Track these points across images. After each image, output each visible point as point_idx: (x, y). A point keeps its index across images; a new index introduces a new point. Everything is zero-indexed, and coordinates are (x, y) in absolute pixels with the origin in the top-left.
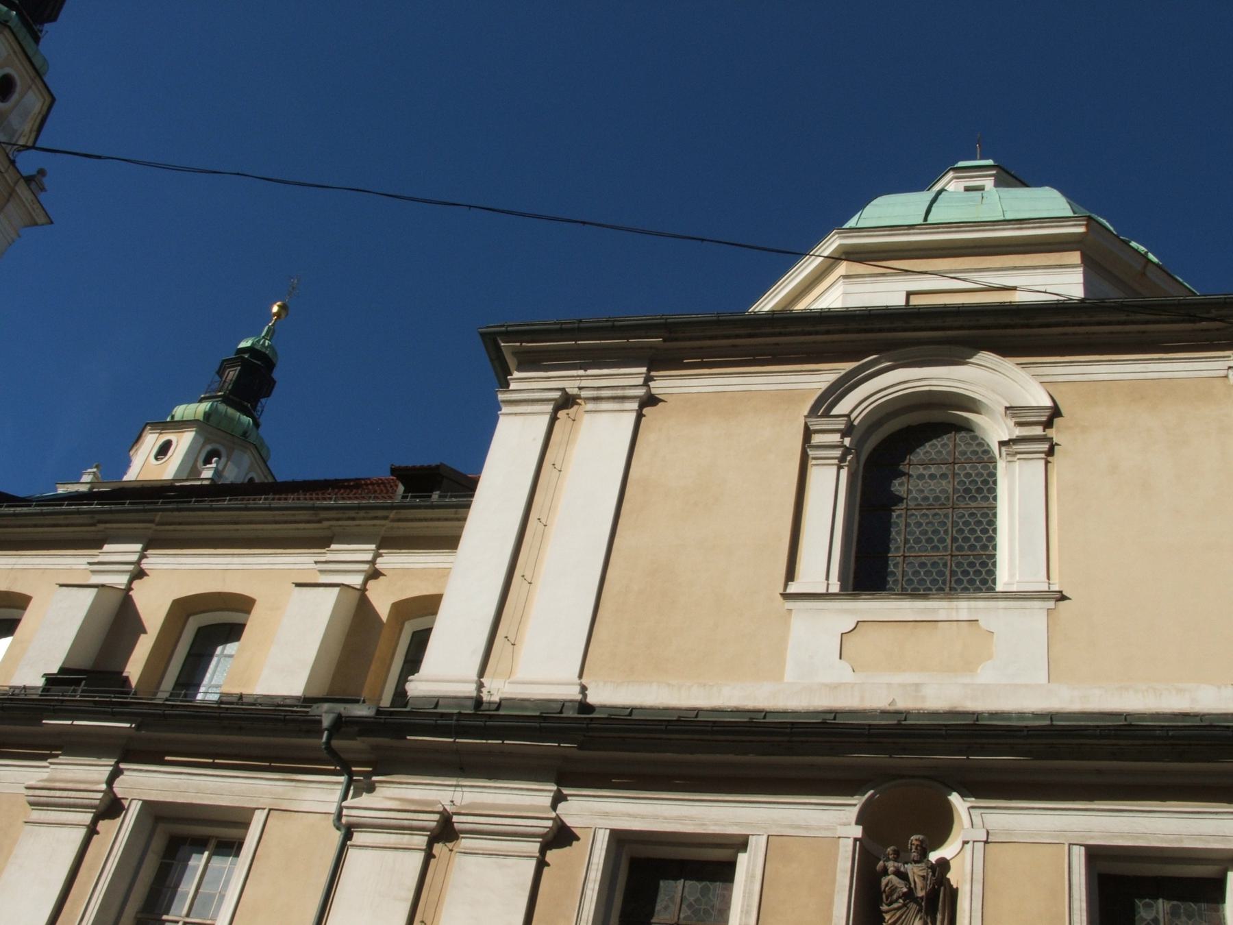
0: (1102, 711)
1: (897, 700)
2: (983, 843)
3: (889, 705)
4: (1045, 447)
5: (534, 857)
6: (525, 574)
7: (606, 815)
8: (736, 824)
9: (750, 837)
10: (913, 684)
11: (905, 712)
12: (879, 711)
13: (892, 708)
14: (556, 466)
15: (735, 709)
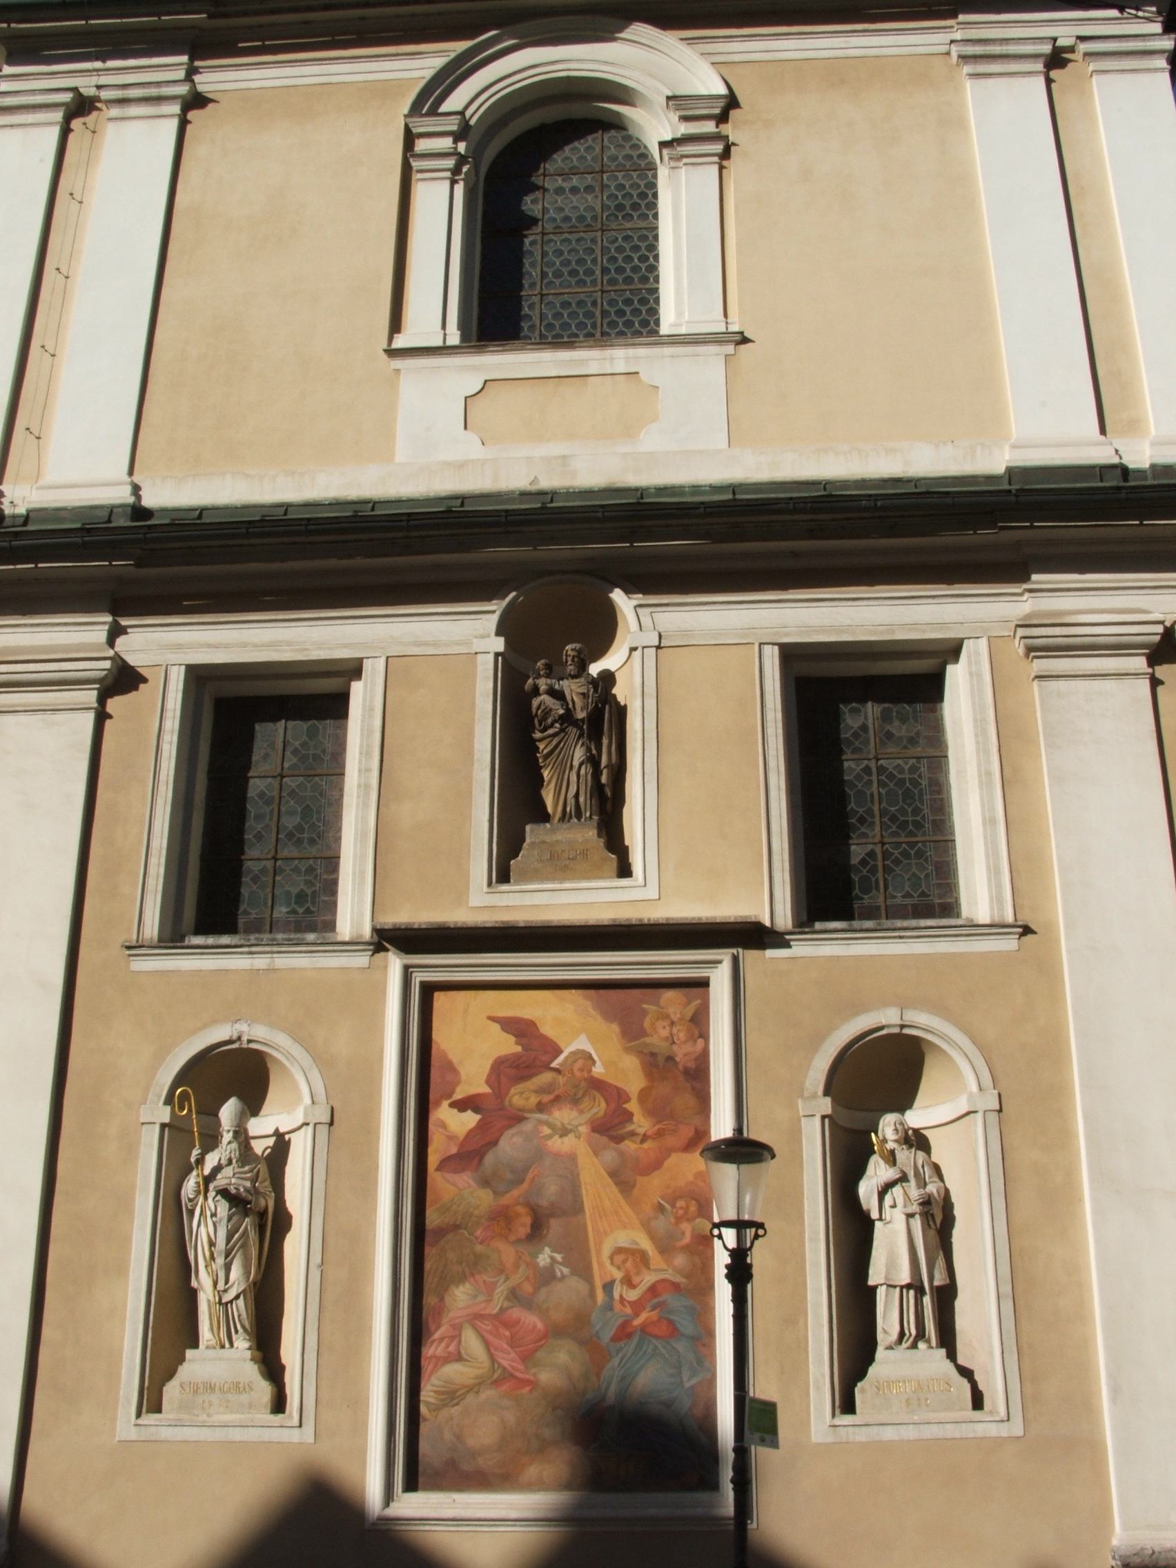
0: (894, 476)
1: (540, 478)
2: (655, 649)
3: (530, 484)
4: (718, 147)
5: (91, 708)
6: (59, 267)
7: (178, 647)
8: (346, 646)
9: (365, 660)
10: (559, 457)
11: (551, 491)
12: (518, 493)
13: (534, 488)
14: (88, 126)
15: (334, 502)
